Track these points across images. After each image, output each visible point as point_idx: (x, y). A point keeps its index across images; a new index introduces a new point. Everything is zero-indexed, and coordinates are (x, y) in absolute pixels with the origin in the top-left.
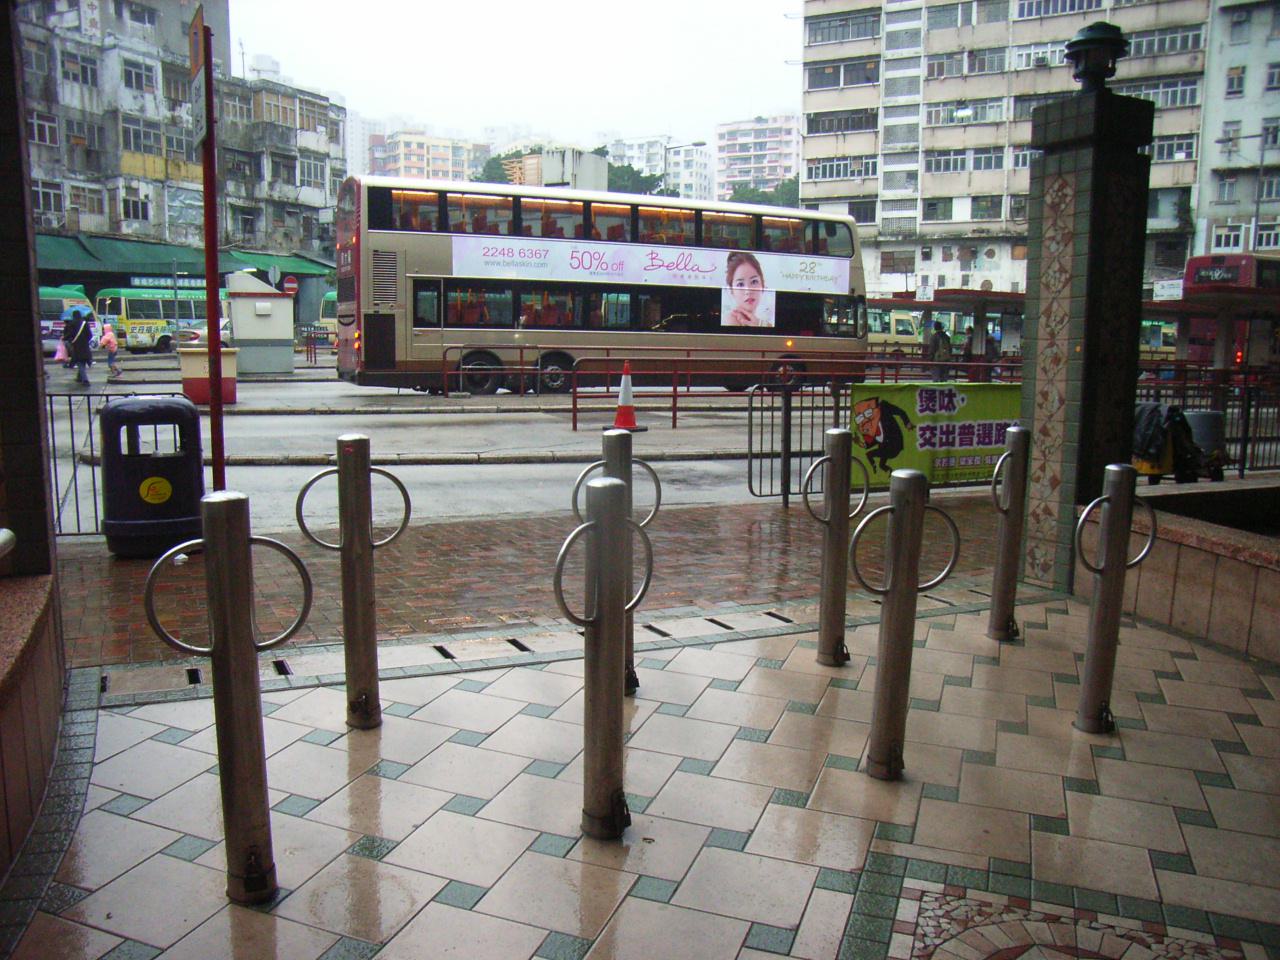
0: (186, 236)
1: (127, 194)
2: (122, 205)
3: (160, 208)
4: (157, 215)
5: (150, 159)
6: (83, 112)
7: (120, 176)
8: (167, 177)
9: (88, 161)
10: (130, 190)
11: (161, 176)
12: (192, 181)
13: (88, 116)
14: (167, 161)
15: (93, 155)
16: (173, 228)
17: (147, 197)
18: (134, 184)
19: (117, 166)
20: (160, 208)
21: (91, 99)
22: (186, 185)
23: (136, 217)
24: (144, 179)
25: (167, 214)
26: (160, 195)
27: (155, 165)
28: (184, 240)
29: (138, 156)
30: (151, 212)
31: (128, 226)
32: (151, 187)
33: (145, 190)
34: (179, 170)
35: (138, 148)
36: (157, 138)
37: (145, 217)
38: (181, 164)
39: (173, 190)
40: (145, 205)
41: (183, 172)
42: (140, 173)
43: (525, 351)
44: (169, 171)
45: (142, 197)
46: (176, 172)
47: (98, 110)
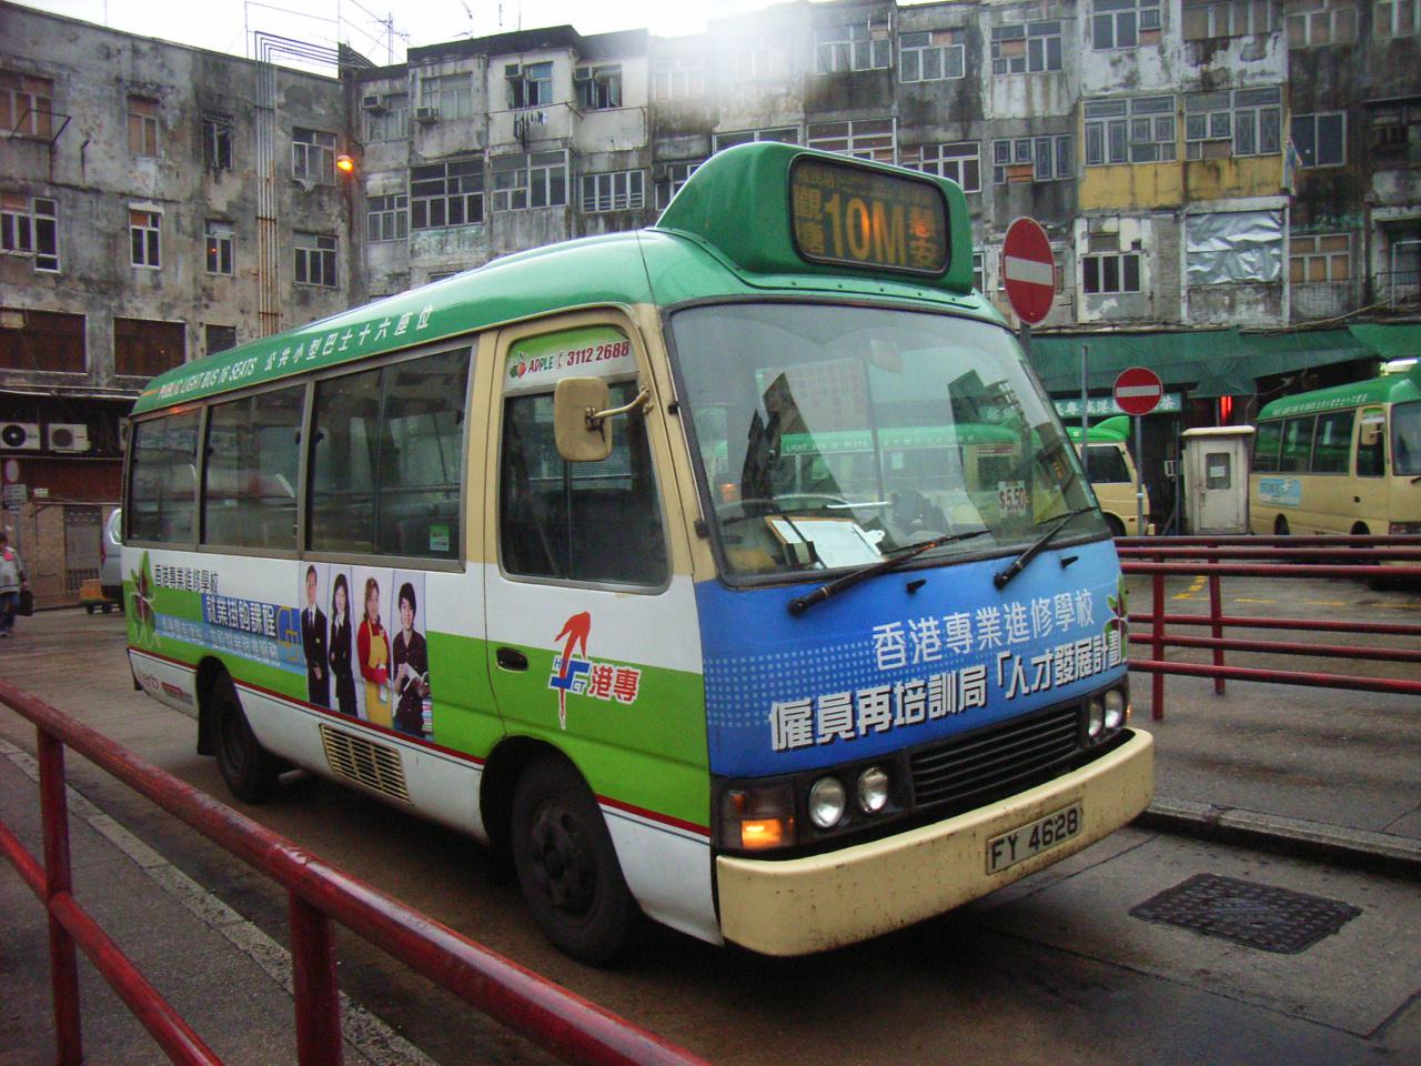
0: (1231, 308)
1: (1092, 249)
2: (1080, 270)
3: (1168, 261)
4: (1159, 278)
5: (1144, 171)
6: (1029, 121)
7: (1079, 216)
8: (1187, 196)
9: (1035, 205)
10: (1099, 238)
11: (1173, 199)
12: (1251, 194)
13: (1038, 125)
14: (1186, 165)
15: (1048, 192)
16: (1197, 298)
17: (1136, 245)
18: (1109, 226)
19: (1075, 202)
20: (1168, 261)
21: (1046, 94)
22: (1234, 204)
23: (1111, 285)
24: (1135, 212)
25: (1185, 269)
26: (1168, 239)
27: (1159, 180)
28: (1224, 316)
29: (1120, 174)
30: (1146, 273)
31: (1091, 308)
32: (1147, 224)
33: (1130, 231)
34: (1218, 177)
35: (1118, 157)
36: (1165, 128)
37: (1133, 282)
38: (1224, 164)
39: (1199, 221)
40: (1132, 264)
41: (1228, 178)
42: (1122, 202)
43: (1168, 678)
44: (1192, 183)
45: (1125, 245)
46: (1211, 184)
47: (1057, 109)
